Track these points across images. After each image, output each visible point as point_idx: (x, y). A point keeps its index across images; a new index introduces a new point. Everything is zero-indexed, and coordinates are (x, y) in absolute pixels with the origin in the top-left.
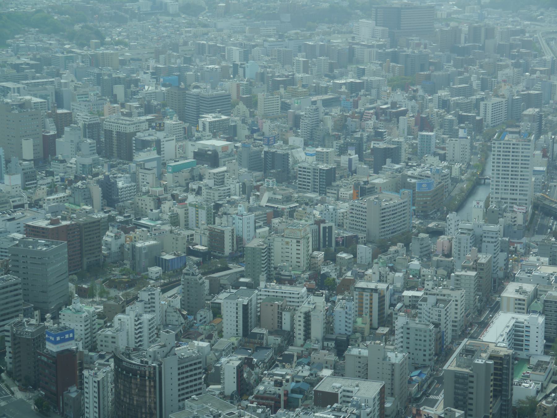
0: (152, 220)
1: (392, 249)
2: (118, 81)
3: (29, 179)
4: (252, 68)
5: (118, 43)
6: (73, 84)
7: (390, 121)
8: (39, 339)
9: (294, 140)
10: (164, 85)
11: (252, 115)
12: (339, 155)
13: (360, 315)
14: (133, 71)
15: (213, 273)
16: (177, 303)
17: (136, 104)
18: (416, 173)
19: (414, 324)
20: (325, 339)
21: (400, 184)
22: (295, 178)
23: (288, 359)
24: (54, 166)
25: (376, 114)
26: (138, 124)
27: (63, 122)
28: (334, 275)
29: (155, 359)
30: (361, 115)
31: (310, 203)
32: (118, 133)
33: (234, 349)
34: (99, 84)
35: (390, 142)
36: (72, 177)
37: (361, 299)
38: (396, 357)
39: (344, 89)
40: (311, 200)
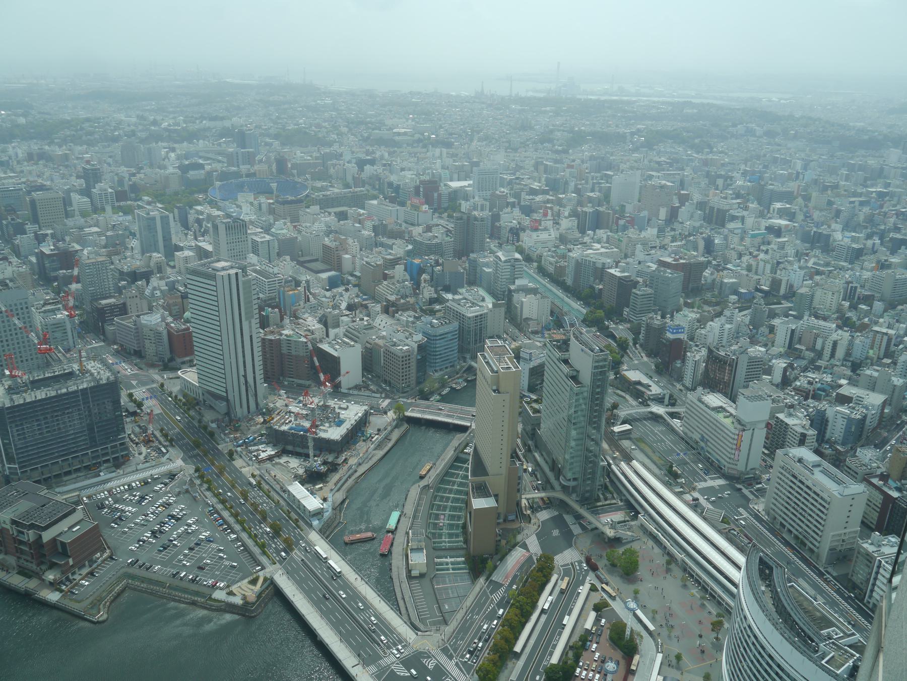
1: (900, 307)
2: (720, 176)
3: (661, 230)
4: (810, 175)
6: (691, 177)
8: (662, 329)
9: (834, 226)
11: (806, 206)
12: (866, 239)
13: (872, 348)
15: (771, 304)
16: (747, 320)
17: (730, 192)
20: (844, 360)
22: (833, 251)
23: (818, 368)
24: (676, 225)
27: (684, 199)
28: (855, 319)
29: (734, 354)
30: (885, 213)
31: (842, 268)
32: (718, 209)
33: (780, 356)
36: (687, 233)
39: (874, 195)
40: (843, 267)
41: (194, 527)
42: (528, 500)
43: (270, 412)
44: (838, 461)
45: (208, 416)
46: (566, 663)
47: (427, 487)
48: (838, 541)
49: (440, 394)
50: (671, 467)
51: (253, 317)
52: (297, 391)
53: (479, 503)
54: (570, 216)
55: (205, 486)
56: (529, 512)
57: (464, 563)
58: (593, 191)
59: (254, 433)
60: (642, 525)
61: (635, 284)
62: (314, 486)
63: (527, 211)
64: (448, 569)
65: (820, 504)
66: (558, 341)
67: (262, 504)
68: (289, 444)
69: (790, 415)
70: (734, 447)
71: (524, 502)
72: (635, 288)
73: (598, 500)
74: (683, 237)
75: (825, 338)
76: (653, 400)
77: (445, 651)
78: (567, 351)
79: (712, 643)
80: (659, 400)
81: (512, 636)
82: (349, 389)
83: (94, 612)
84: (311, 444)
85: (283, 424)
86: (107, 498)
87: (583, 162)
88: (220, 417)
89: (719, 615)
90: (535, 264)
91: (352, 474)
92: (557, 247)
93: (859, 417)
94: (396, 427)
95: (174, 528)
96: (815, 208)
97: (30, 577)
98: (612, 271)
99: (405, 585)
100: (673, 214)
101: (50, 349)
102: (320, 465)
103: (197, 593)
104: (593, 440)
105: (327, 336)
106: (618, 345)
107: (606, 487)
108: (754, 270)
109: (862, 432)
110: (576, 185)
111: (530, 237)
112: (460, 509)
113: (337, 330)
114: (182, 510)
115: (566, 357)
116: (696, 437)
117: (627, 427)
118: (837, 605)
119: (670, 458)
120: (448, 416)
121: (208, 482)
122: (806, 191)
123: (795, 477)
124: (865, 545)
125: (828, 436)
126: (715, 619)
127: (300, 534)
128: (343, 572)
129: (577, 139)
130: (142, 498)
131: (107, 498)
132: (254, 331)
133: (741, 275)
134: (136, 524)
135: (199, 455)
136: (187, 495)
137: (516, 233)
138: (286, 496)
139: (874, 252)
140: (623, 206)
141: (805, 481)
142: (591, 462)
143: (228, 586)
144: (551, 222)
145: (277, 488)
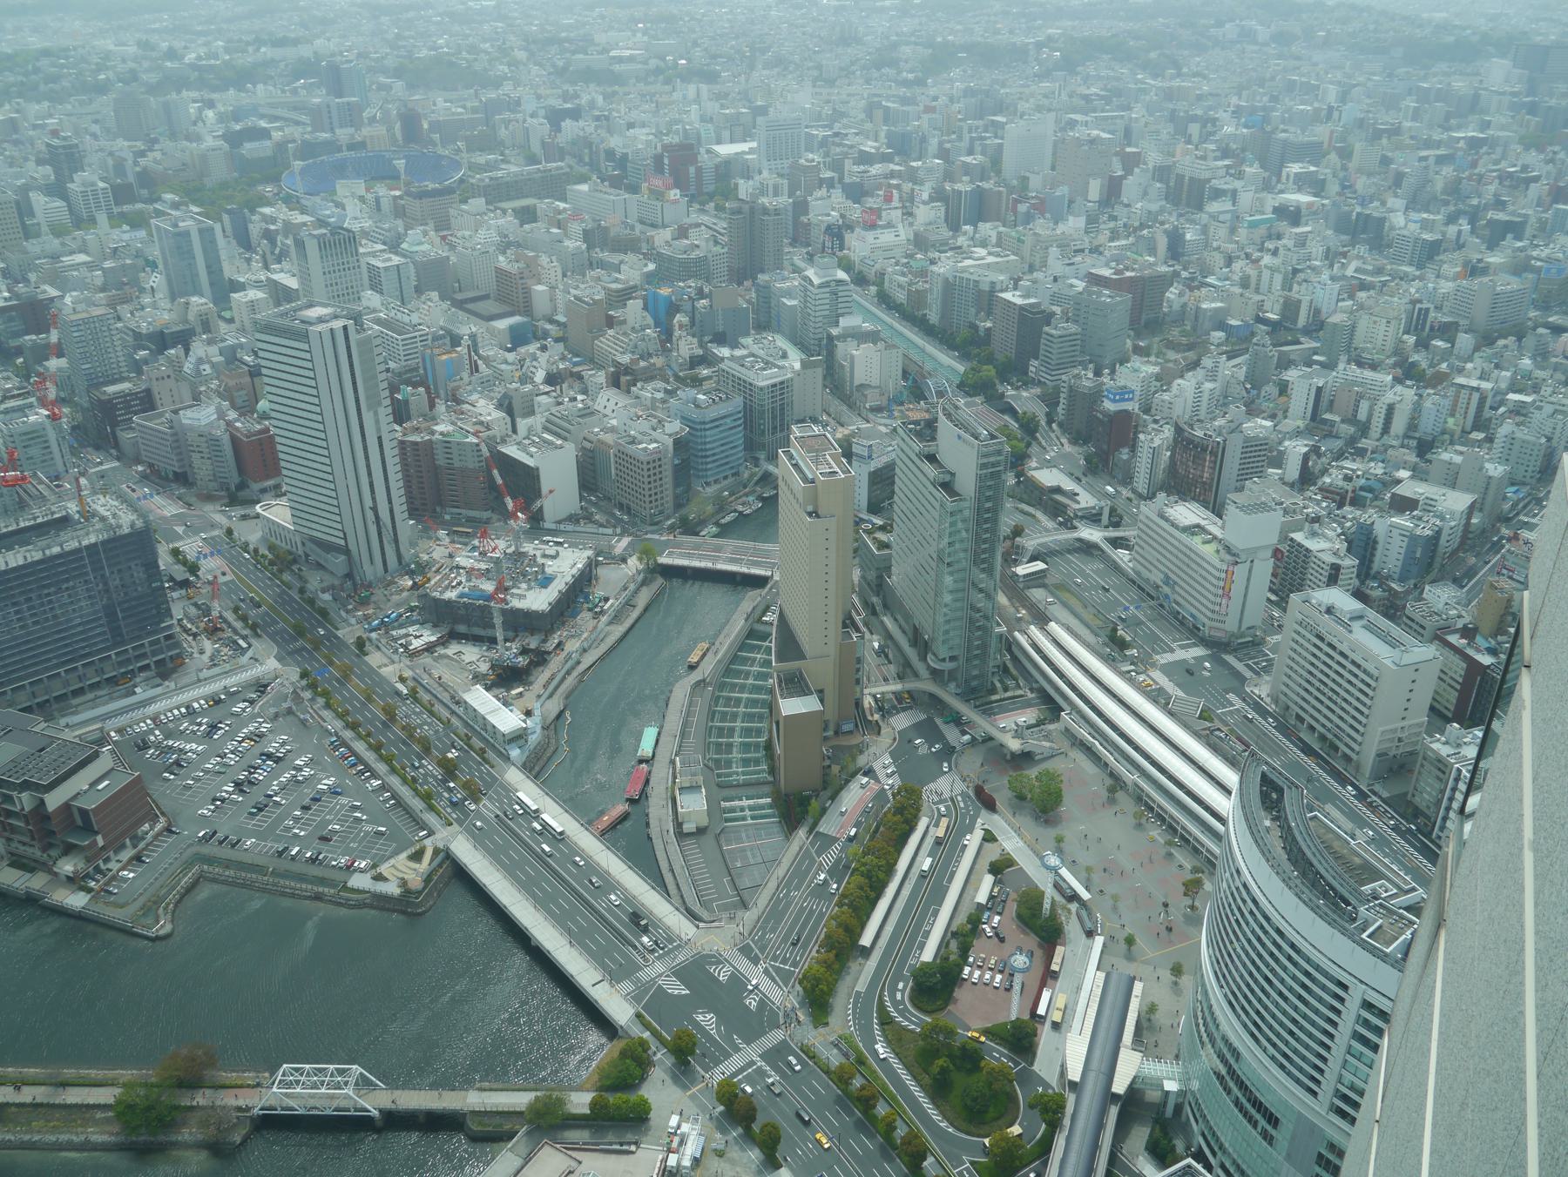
0: (1219, 279)
1: (1501, 342)
2: (1194, 119)
3: (1092, 220)
4: (1351, 111)
5: (1196, 75)
7: (1515, 187)
8: (1096, 396)
10: (1246, 126)
11: (1344, 168)
12: (1447, 224)
13: (1452, 415)
14: (1210, 108)
16: (1241, 374)
17: (1213, 147)
18: (1543, 255)
19: (1522, 434)
20: (1406, 436)
21: (1520, 267)
22: (1389, 246)
23: (1361, 453)
24: (1119, 211)
25: (1500, 177)
26: (1214, 169)
27: (1131, 162)
28: (1424, 365)
30: (1481, 176)
31: (1404, 277)
32: (1191, 179)
33: (1298, 434)
34: (1172, 120)
35: (1513, 213)
36: (1137, 224)
37: (1457, 397)
38: (1495, 470)
40: (1406, 274)
41: (307, 772)
42: (874, 696)
43: (422, 568)
44: (1392, 609)
45: (314, 581)
46: (947, 959)
47: (701, 684)
48: (1391, 740)
49: (717, 524)
50: (1115, 630)
51: (380, 404)
52: (471, 529)
53: (791, 706)
54: (932, 199)
55: (321, 701)
56: (876, 717)
57: (770, 806)
58: (970, 152)
59: (398, 605)
60: (1067, 730)
61: (1048, 318)
62: (508, 691)
63: (856, 193)
64: (744, 819)
65: (1363, 681)
66: (916, 423)
67: (420, 726)
68: (460, 622)
69: (1314, 534)
70: (1220, 592)
71: (868, 701)
72: (1048, 324)
73: (993, 691)
74: (1130, 230)
75: (1374, 401)
76: (1082, 518)
77: (745, 951)
78: (934, 439)
79: (1185, 915)
80: (1093, 518)
81: (854, 922)
82: (559, 522)
83: (149, 921)
84: (498, 620)
85: (447, 588)
86: (151, 731)
87: (952, 100)
88: (337, 583)
89: (1195, 870)
90: (873, 289)
91: (573, 668)
92: (911, 256)
93: (1429, 533)
94: (644, 583)
95: (273, 775)
96: (1359, 171)
97: (32, 870)
98: (1007, 296)
99: (674, 847)
100: (1113, 189)
101: (23, 479)
102: (516, 656)
103: (322, 881)
104: (981, 590)
105: (515, 431)
106: (1021, 426)
107: (1006, 670)
108: (1253, 285)
109: (1432, 558)
110: (941, 143)
111: (863, 240)
112: (761, 717)
113: (530, 420)
114: (283, 744)
115: (932, 450)
116: (1156, 577)
117: (1040, 566)
118: (1389, 844)
119: (1112, 616)
120: (732, 561)
121: (325, 694)
122: (1343, 140)
123: (1322, 639)
124: (1435, 746)
125: (1376, 567)
126: (1190, 877)
127: (489, 773)
128: (568, 832)
129: (940, 59)
130: (214, 727)
131: (151, 731)
132: (385, 429)
133: (1230, 295)
134: (206, 772)
135: (304, 648)
136: (290, 718)
137: (837, 233)
138: (460, 711)
139: (1460, 246)
140: (1025, 179)
141: (1338, 645)
142: (979, 628)
143: (374, 866)
144: (899, 212)
145: (445, 697)
